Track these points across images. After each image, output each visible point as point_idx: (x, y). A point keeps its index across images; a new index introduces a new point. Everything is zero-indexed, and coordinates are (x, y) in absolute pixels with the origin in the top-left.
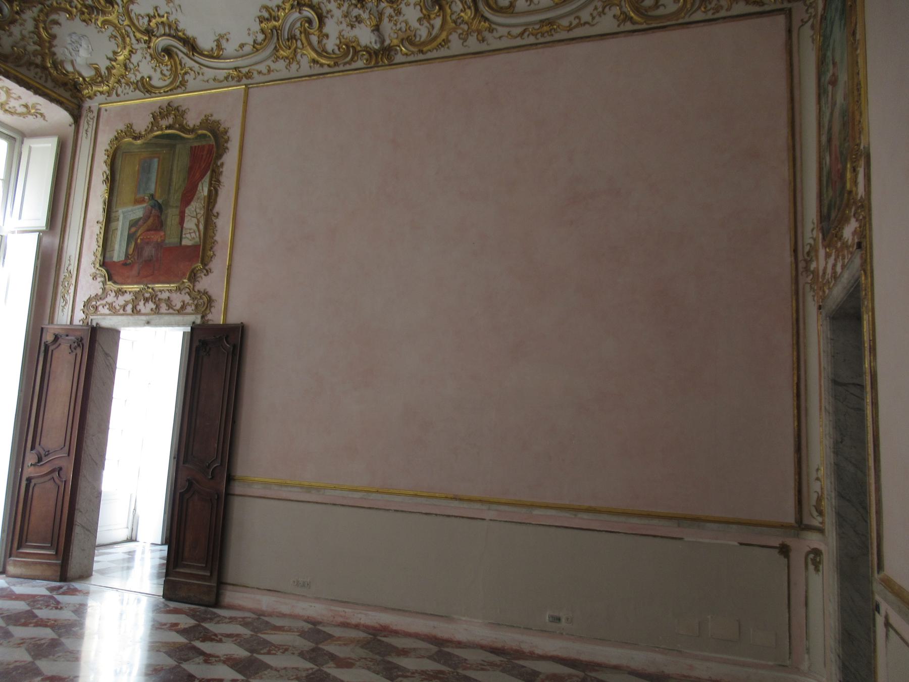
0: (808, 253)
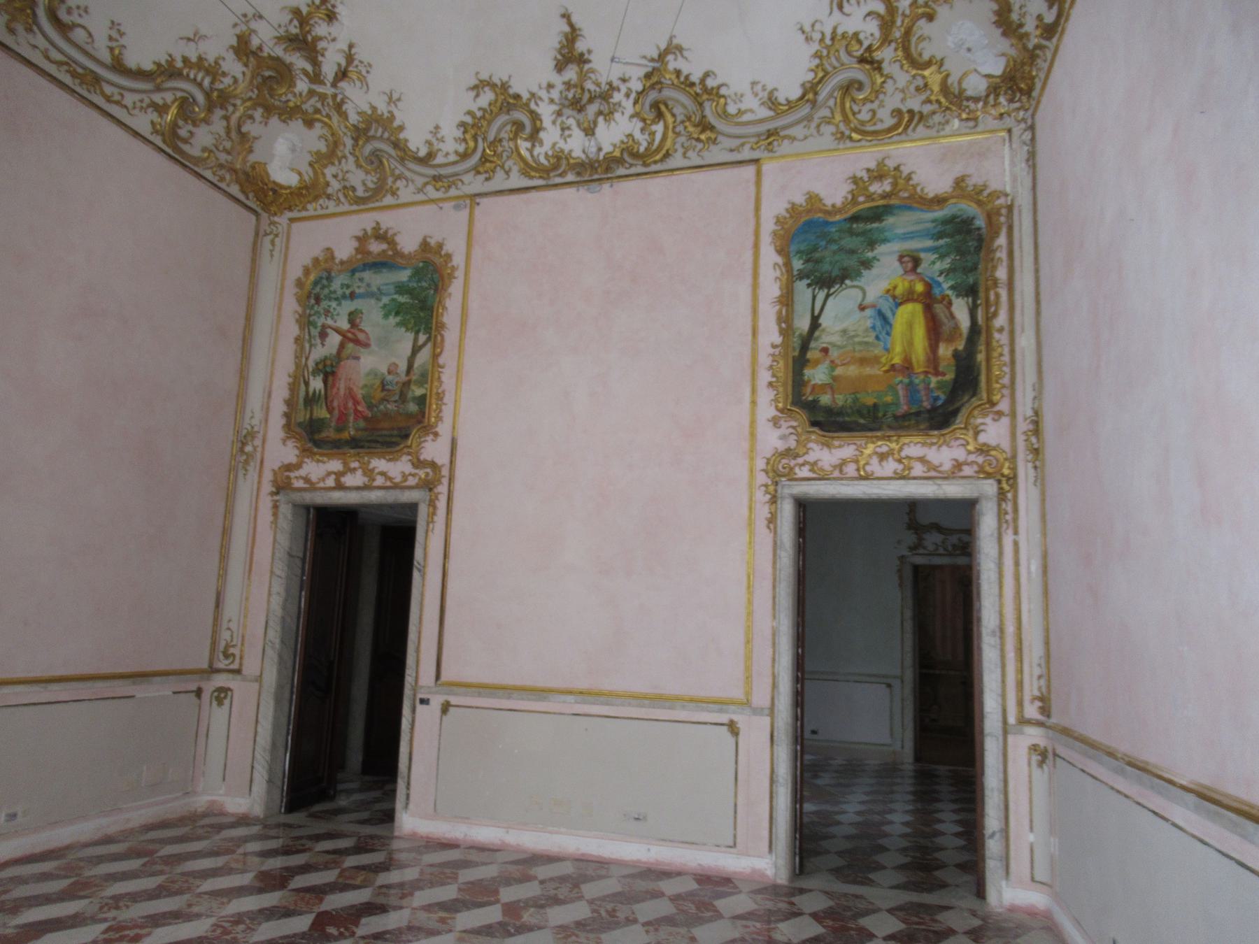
0: (245, 437)
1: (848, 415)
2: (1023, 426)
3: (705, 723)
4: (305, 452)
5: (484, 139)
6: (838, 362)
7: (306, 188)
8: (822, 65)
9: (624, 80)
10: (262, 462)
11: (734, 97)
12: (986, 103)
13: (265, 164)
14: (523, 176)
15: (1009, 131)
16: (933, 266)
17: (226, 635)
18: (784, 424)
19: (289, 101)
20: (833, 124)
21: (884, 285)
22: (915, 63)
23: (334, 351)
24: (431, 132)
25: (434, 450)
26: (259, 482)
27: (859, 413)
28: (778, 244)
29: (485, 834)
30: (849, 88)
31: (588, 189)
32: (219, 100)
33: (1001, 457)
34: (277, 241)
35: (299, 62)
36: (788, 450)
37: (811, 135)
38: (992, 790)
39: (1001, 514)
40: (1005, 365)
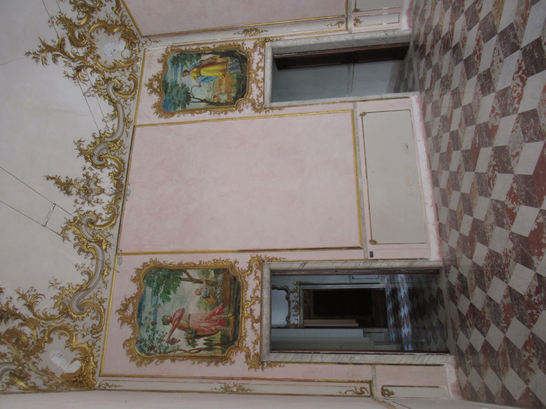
1: (240, 87)
2: (248, 37)
3: (363, 124)
6: (219, 92)
9: (84, 169)
10: (244, 379)
13: (63, 373)
14: (114, 228)
16: (188, 66)
17: (349, 393)
18: (242, 107)
23: (183, 332)
24: (78, 270)
26: (256, 379)
29: (430, 214)
30: (116, 89)
33: (258, 42)
34: (110, 383)
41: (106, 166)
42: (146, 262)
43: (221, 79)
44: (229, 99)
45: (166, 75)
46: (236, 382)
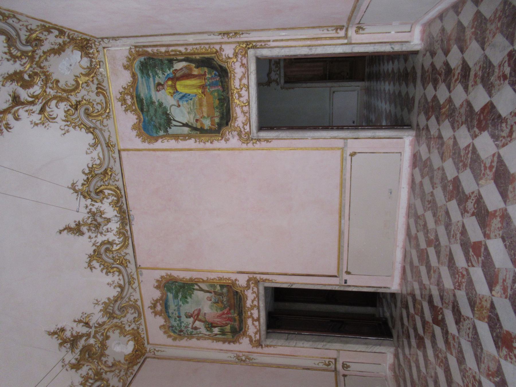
0: (239, 360)
1: (223, 110)
2: (225, 39)
3: (351, 166)
4: (245, 334)
5: (113, 264)
6: (201, 115)
7: (135, 338)
8: (78, 125)
9: (87, 207)
11: (92, 162)
12: (93, 58)
15: (104, 48)
16: (161, 78)
17: (321, 365)
19: (98, 346)
20: (103, 120)
21: (169, 97)
22: (77, 87)
23: (203, 324)
24: (110, 286)
25: (242, 280)
26: (257, 353)
27: (222, 106)
28: (153, 141)
29: (399, 255)
30: (88, 114)
31: (133, 220)
32: (98, 376)
34: (157, 349)
35: (82, 343)
36: (238, 134)
37: (108, 129)
38: (374, 49)
39: (262, 47)
40: (201, 47)
41: (105, 197)
42: (162, 275)
43: (201, 98)
44: (213, 125)
45: (137, 87)
46: (244, 353)
